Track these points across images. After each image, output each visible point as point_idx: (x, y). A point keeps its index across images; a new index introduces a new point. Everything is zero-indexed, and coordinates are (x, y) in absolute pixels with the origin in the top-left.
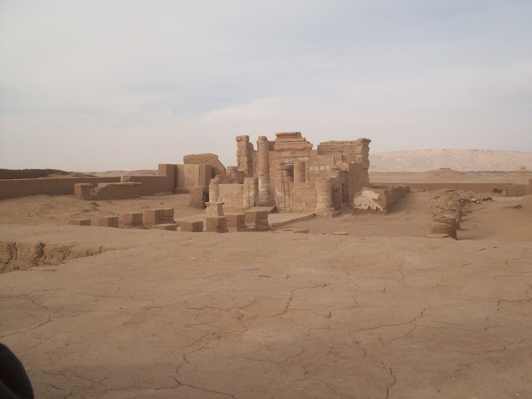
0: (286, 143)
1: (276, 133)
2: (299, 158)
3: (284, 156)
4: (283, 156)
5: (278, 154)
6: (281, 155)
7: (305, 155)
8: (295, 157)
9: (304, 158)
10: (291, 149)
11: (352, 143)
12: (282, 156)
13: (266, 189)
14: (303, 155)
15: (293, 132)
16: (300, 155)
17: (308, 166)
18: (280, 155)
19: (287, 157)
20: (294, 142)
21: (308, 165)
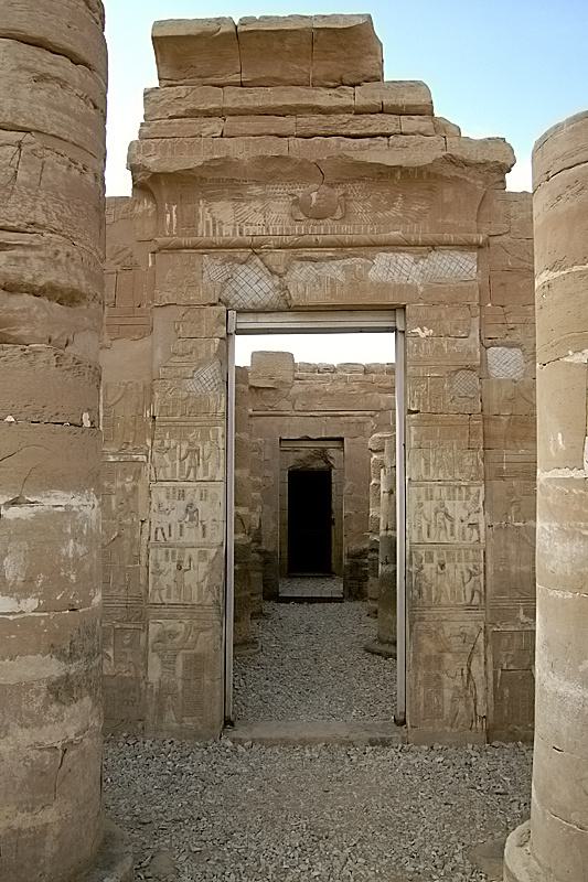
0: (244, 124)
1: (158, 25)
2: (382, 258)
3: (228, 233)
4: (218, 240)
5: (172, 216)
6: (201, 226)
7: (447, 237)
8: (342, 247)
9: (434, 256)
10: (306, 171)
11: (367, 370)
12: (203, 233)
13: (31, 604)
14: (421, 232)
15: (335, 17)
16: (395, 234)
17: (475, 335)
18: (190, 223)
19: (255, 248)
20: (334, 119)
21: (476, 322)
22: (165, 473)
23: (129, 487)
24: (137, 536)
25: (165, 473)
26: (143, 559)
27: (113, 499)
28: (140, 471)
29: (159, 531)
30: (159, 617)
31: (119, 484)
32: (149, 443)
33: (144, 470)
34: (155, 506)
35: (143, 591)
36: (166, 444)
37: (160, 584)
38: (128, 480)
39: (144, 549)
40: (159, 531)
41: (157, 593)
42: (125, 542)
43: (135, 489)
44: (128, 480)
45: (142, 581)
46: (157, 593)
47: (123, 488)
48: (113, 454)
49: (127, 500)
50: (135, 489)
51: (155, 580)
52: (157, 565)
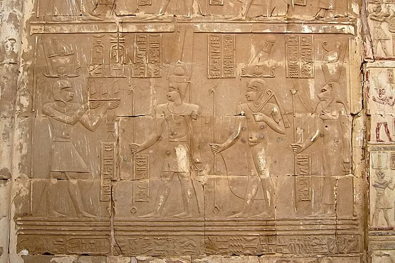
22: (384, 48)
23: (332, 68)
24: (347, 135)
25: (384, 48)
26: (358, 167)
27: (311, 83)
28: (347, 47)
29: (382, 127)
30: (385, 247)
31: (318, 64)
32: (355, 9)
33: (352, 45)
34: (373, 93)
35: (358, 211)
36: (384, 10)
37: (386, 202)
38: (330, 58)
39: (358, 153)
40: (382, 127)
41: (381, 214)
42: (332, 143)
43: (341, 70)
44: (330, 58)
45: (358, 198)
46: (381, 214)
47: (324, 70)
48: (308, 23)
49: (331, 86)
50: (341, 70)
51: (379, 196)
52: (381, 175)
